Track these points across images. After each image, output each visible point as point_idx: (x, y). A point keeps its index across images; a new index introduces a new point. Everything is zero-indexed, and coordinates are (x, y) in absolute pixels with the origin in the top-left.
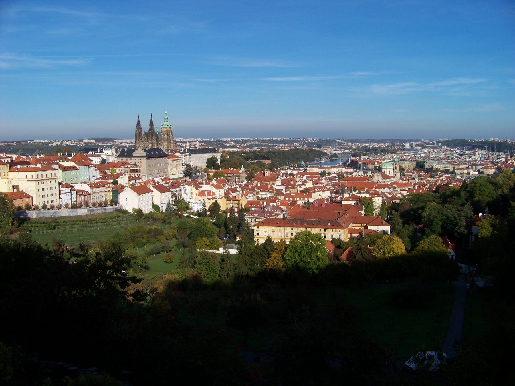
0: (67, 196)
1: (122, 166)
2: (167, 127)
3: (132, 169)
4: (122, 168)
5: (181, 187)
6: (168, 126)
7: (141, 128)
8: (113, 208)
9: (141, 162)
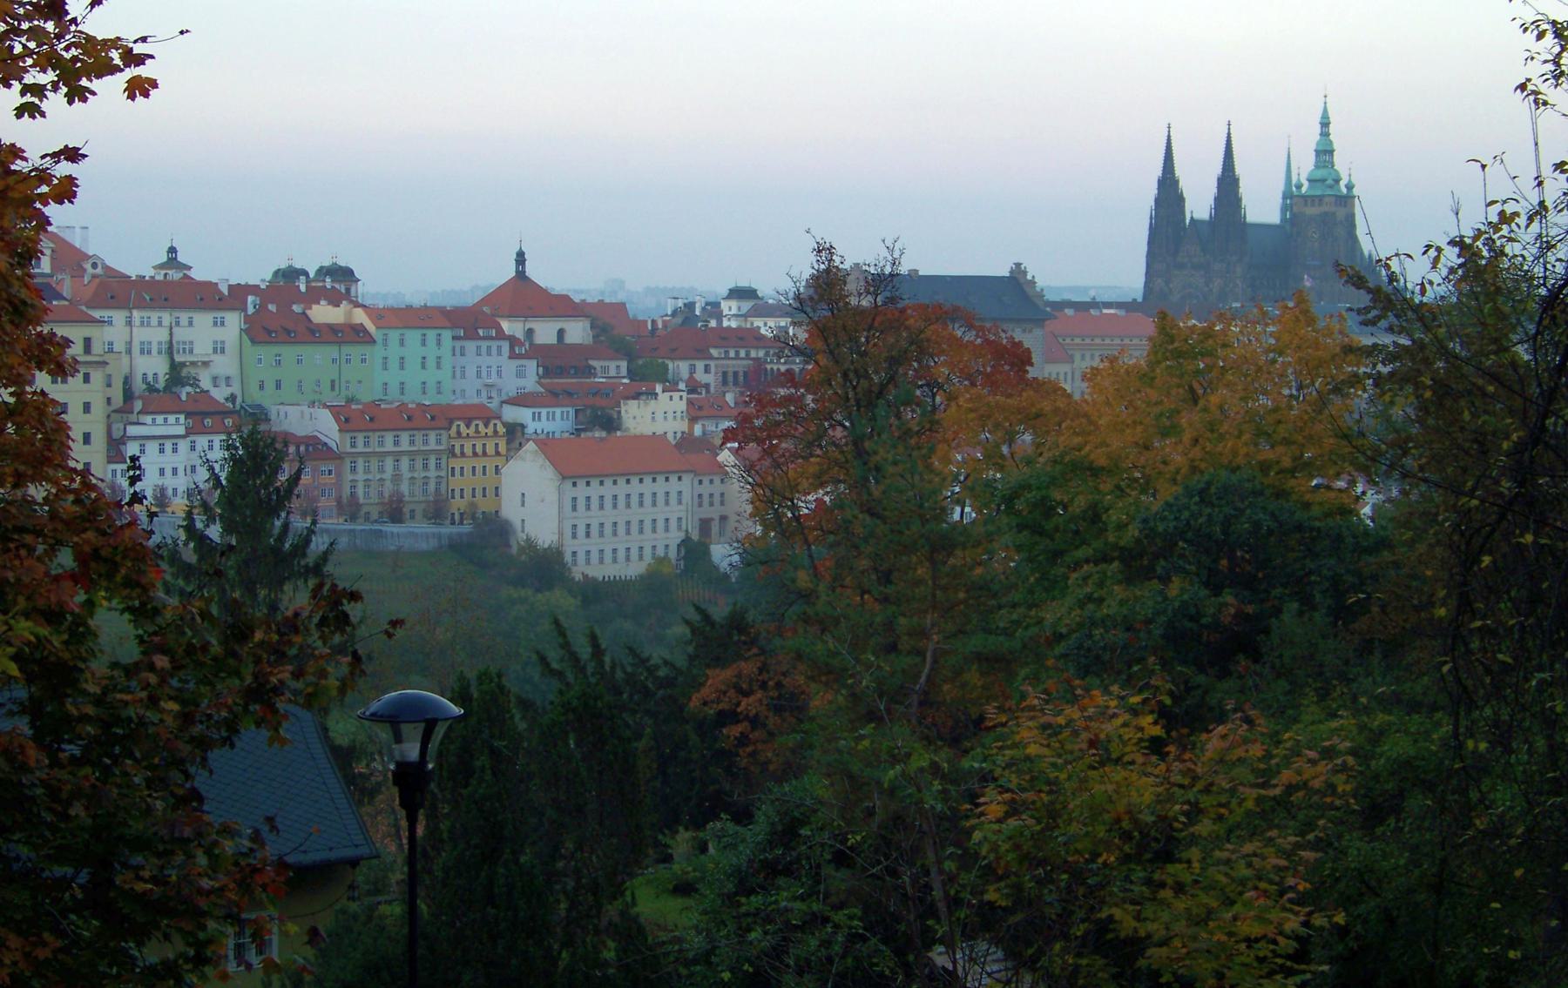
0: (162, 451)
1: (714, 352)
2: (1321, 198)
3: (769, 367)
4: (711, 358)
6: (1329, 192)
8: (439, 536)
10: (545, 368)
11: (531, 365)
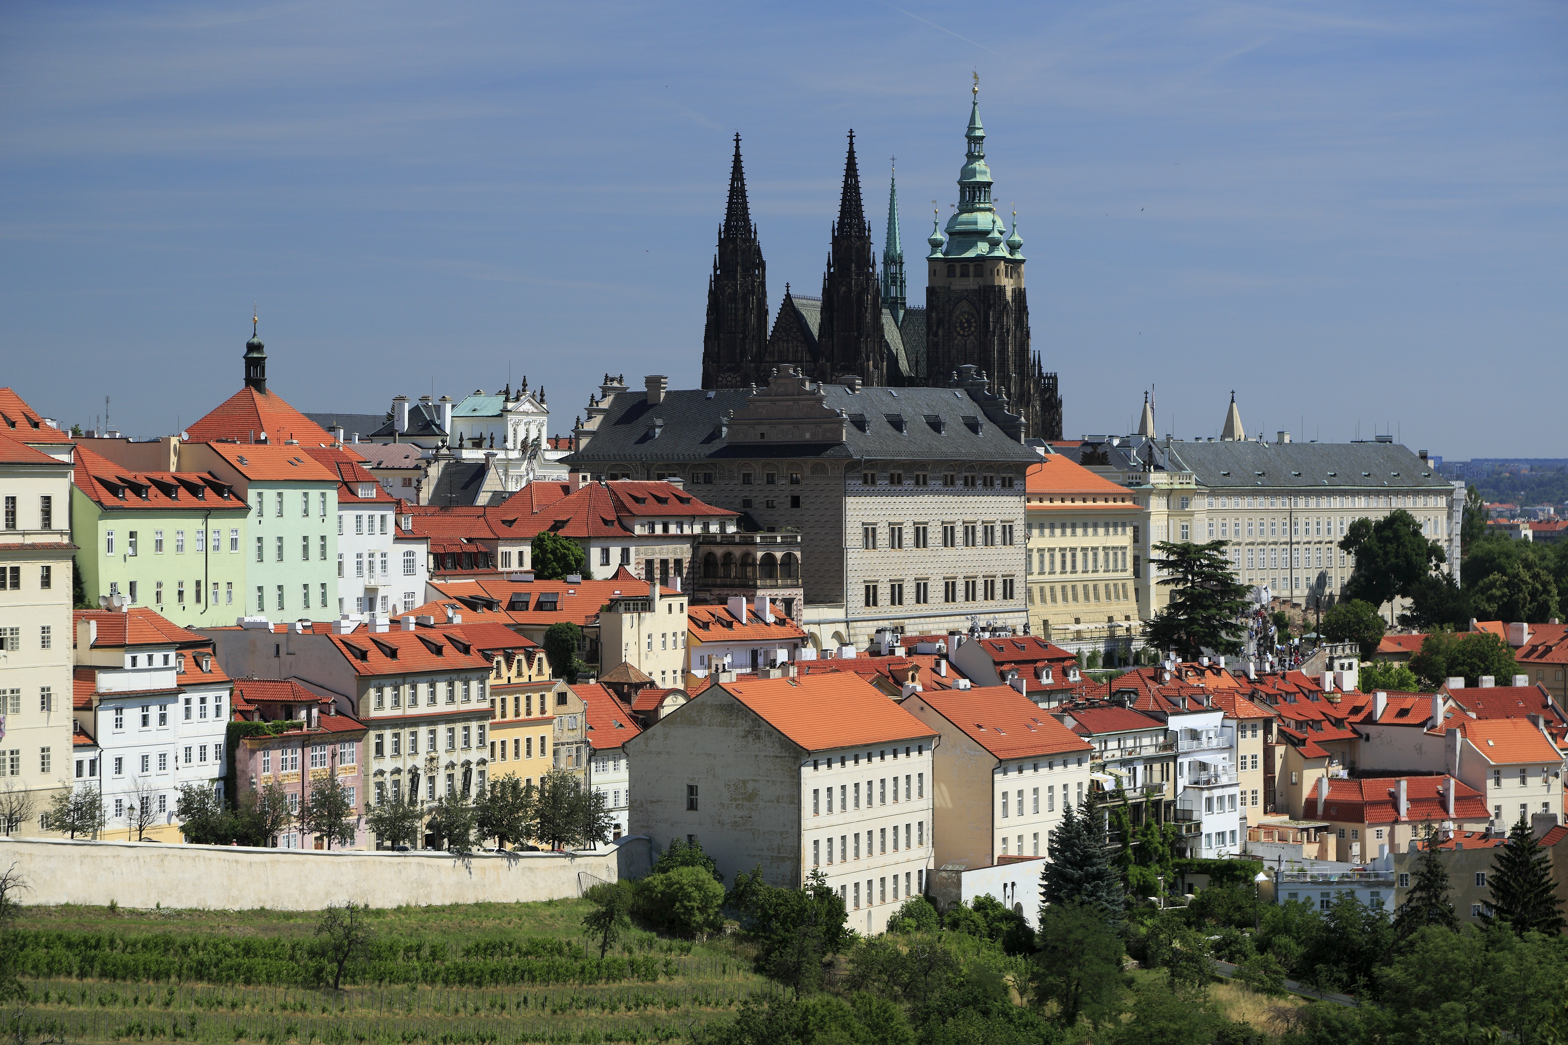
0: (145, 721)
3: (719, 551)
5: (1175, 723)
7: (762, 265)
9: (796, 502)
10: (437, 557)
11: (421, 551)
